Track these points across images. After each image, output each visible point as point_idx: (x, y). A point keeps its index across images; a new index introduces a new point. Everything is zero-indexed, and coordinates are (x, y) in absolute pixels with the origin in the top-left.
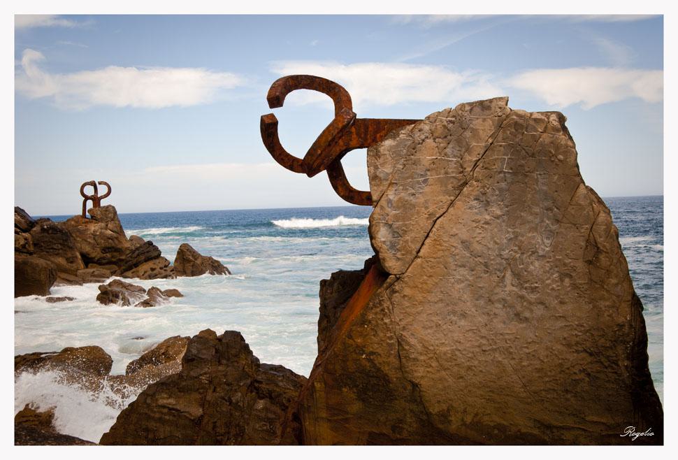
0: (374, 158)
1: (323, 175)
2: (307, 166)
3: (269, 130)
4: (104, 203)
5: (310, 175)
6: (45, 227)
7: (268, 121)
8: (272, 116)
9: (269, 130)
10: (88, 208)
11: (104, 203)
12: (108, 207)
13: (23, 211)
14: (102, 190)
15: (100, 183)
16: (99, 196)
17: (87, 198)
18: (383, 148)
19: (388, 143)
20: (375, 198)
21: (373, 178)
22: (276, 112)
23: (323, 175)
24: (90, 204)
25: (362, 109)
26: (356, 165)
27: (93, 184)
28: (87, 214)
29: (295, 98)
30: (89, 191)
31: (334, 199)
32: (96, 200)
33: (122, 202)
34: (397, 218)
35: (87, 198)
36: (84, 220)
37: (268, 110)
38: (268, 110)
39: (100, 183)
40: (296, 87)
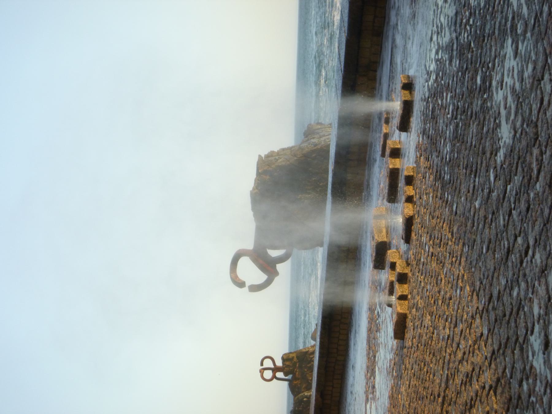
3: (255, 288)
4: (279, 363)
5: (276, 273)
9: (255, 288)
12: (283, 359)
14: (268, 363)
15: (262, 364)
16: (272, 366)
17: (274, 377)
22: (248, 284)
24: (280, 375)
25: (249, 245)
26: (274, 253)
27: (262, 371)
28: (287, 378)
30: (268, 374)
32: (275, 369)
33: (279, 348)
35: (274, 377)
37: (246, 289)
38: (246, 289)
39: (262, 364)
40: (237, 276)
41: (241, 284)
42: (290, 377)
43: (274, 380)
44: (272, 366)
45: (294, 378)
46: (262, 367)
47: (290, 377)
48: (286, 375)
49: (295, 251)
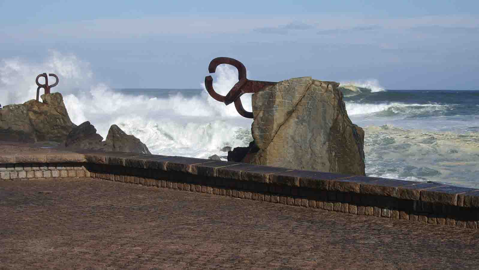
0: (254, 98)
1: (233, 105)
2: (227, 100)
4: (52, 91)
5: (227, 104)
7: (208, 79)
8: (210, 76)
10: (40, 94)
11: (52, 91)
12: (57, 93)
14: (52, 81)
15: (50, 75)
16: (49, 84)
17: (40, 86)
18: (259, 95)
19: (260, 93)
20: (254, 116)
21: (254, 107)
23: (233, 105)
24: (42, 91)
26: (246, 101)
27: (45, 75)
29: (220, 68)
30: (42, 81)
31: (236, 114)
32: (47, 88)
34: (264, 125)
35: (40, 86)
38: (208, 74)
39: (50, 75)
41: (212, 68)
42: (41, 100)
43: (38, 87)
44: (49, 84)
46: (48, 77)
47: (41, 100)
49: (252, 120)
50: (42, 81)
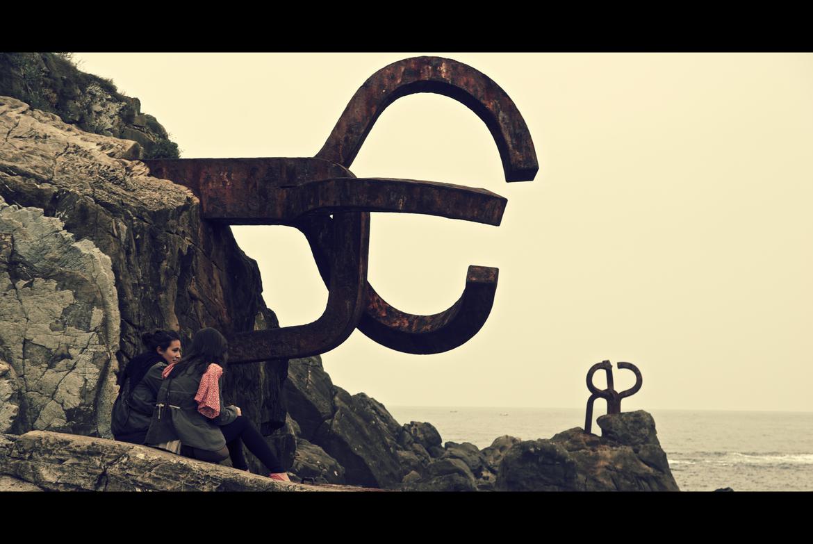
4: (627, 405)
6: (532, 450)
11: (627, 405)
13: (381, 405)
14: (624, 380)
15: (621, 365)
17: (596, 393)
24: (601, 406)
27: (606, 366)
30: (600, 381)
32: (614, 399)
35: (596, 393)
36: (588, 438)
39: (621, 365)
42: (596, 430)
43: (590, 394)
44: (619, 388)
45: (595, 442)
46: (615, 370)
48: (600, 421)
50: (600, 381)
